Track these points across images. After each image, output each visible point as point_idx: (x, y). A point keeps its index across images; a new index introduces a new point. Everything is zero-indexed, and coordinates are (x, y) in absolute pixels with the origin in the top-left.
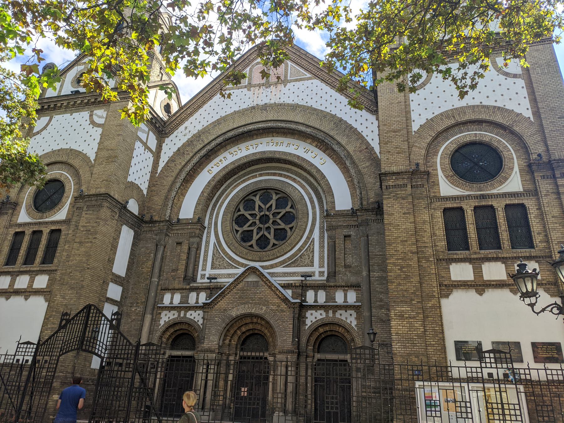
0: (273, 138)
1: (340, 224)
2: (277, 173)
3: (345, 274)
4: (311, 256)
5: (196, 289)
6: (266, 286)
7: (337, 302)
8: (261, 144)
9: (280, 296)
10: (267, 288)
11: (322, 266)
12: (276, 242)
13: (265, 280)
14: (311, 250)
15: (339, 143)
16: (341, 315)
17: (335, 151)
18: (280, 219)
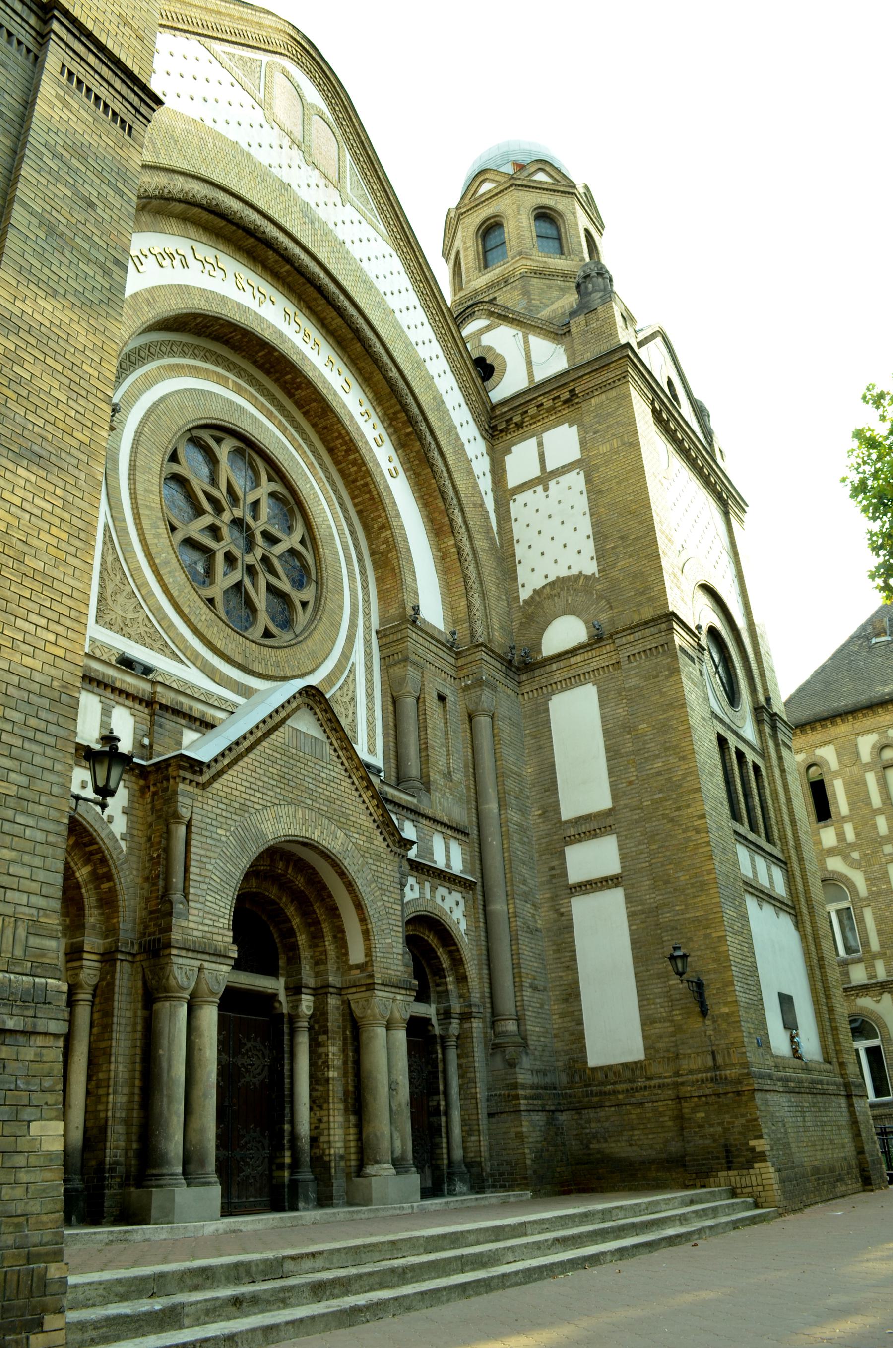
0: (298, 312)
1: (430, 657)
2: (276, 417)
3: (445, 794)
4: (351, 712)
5: (99, 683)
6: (340, 766)
7: (435, 862)
8: (273, 302)
9: (372, 811)
10: (343, 772)
11: (371, 751)
12: (273, 629)
13: (336, 745)
14: (350, 696)
15: (442, 454)
16: (443, 899)
17: (432, 466)
18: (280, 557)
